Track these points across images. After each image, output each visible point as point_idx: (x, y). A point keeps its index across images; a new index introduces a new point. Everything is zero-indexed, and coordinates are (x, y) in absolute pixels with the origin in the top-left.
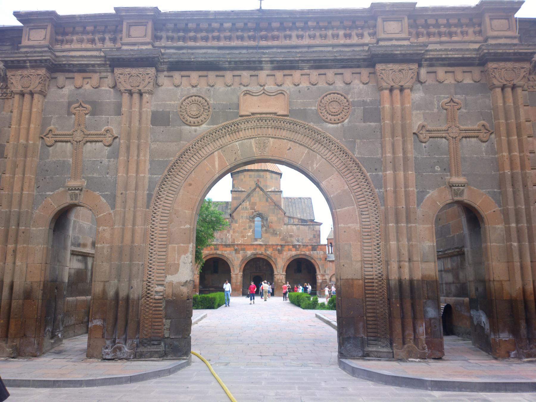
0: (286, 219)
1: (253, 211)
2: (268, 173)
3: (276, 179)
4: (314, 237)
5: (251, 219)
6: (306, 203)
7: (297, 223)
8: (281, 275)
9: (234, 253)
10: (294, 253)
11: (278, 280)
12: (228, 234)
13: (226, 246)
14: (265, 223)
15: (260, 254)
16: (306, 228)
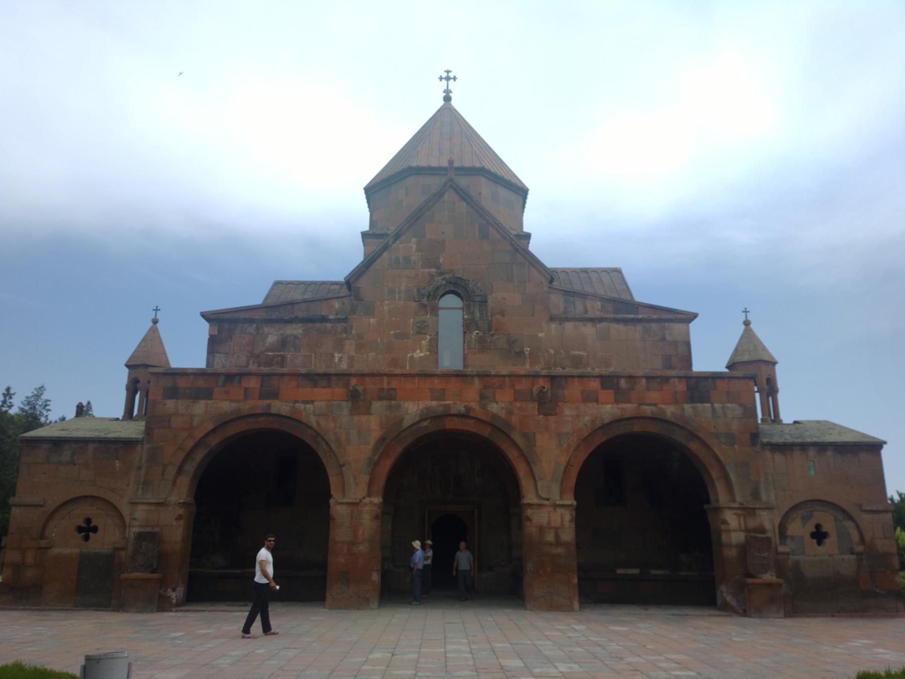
1: (433, 270)
2: (483, 180)
4: (668, 364)
5: (425, 301)
7: (598, 314)
8: (556, 506)
9: (346, 411)
10: (608, 410)
11: (541, 529)
12: (337, 356)
14: (477, 314)
15: (459, 416)
16: (635, 332)
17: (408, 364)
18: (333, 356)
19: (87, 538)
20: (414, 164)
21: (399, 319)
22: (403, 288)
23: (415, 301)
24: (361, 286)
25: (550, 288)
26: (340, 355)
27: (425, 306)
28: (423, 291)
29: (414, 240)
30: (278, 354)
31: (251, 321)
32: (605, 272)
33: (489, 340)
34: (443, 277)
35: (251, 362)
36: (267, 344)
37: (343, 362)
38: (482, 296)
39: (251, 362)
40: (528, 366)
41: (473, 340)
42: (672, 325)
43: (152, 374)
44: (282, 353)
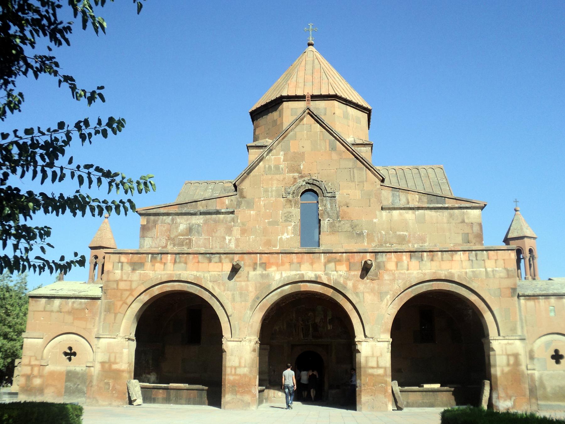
0: (387, 197)
1: (296, 175)
2: (336, 103)
3: (358, 121)
5: (290, 197)
6: (431, 176)
7: (417, 204)
11: (367, 357)
12: (228, 238)
13: (209, 255)
14: (329, 206)
17: (278, 244)
18: (226, 239)
19: (70, 359)
20: (285, 94)
21: (271, 211)
22: (274, 188)
23: (283, 198)
24: (244, 188)
25: (381, 185)
26: (230, 238)
27: (290, 201)
28: (289, 190)
29: (282, 153)
30: (187, 237)
31: (168, 214)
32: (432, 169)
33: (337, 225)
34: (303, 179)
35: (169, 243)
36: (179, 231)
37: (232, 243)
38: (332, 193)
39: (169, 243)
40: (366, 244)
41: (326, 225)
42: (469, 211)
43: (106, 253)
44: (189, 237)
